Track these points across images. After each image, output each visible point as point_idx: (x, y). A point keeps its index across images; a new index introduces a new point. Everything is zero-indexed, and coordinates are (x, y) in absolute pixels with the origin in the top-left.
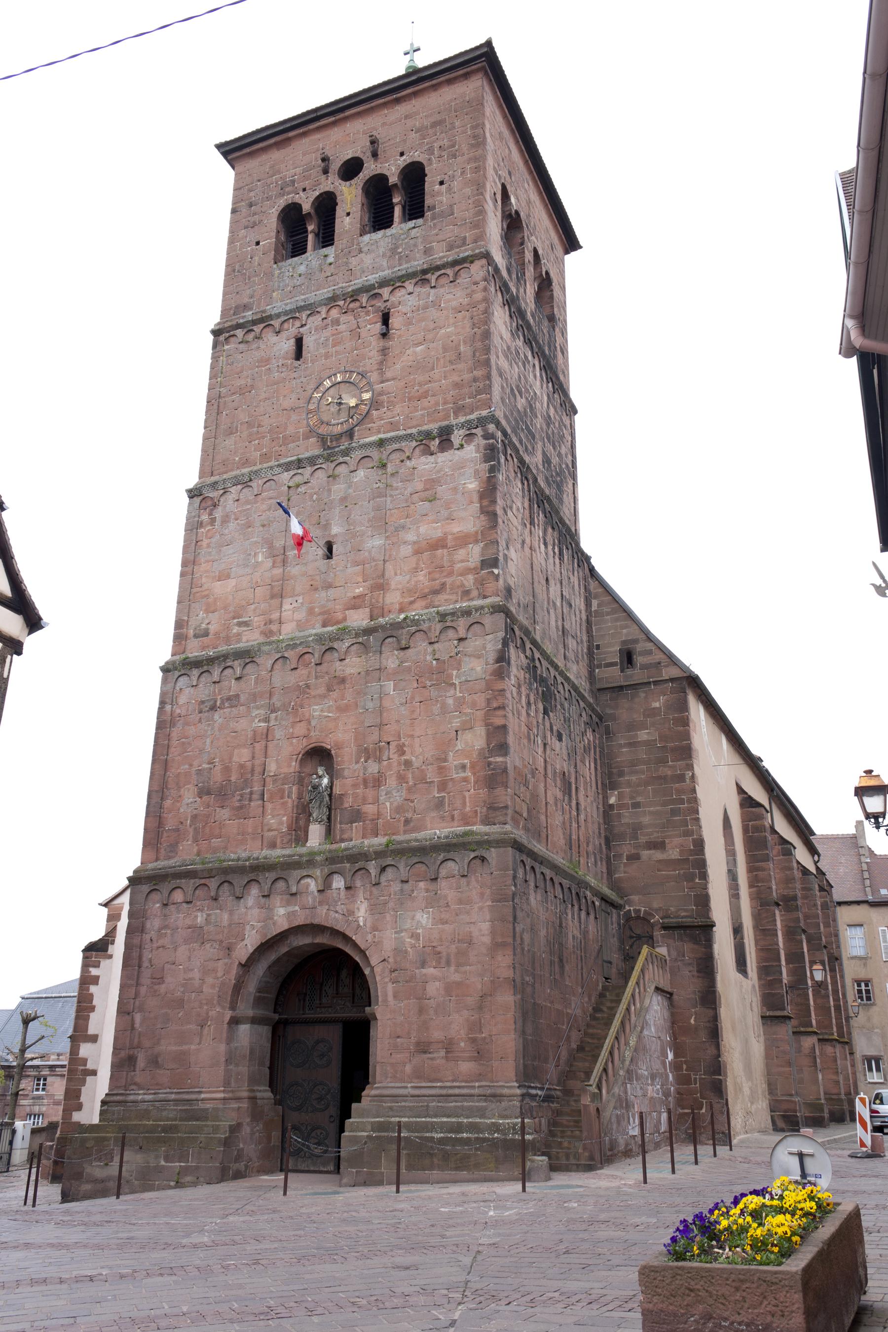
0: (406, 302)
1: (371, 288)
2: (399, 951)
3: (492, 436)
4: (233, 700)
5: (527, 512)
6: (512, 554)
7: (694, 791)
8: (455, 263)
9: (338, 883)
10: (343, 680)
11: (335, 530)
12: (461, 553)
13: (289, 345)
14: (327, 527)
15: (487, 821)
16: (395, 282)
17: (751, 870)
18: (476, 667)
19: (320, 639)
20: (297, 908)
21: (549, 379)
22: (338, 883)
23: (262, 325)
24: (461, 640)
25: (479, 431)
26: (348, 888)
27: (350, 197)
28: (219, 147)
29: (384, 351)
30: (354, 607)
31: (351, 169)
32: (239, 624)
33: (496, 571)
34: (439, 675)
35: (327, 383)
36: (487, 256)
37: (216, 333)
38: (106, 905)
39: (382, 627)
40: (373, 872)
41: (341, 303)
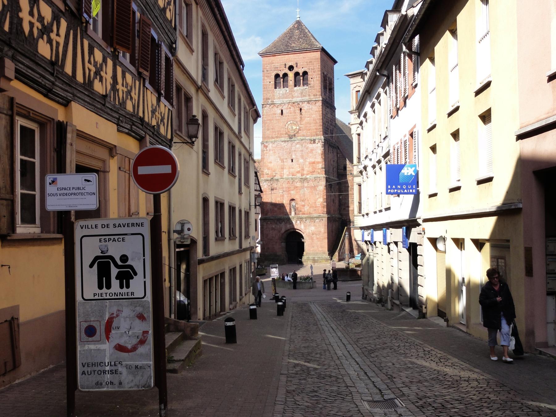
0: (305, 106)
2: (309, 233)
11: (294, 157)
12: (318, 165)
14: (291, 156)
16: (303, 102)
19: (292, 179)
22: (298, 222)
27: (291, 75)
29: (301, 118)
31: (291, 68)
34: (315, 187)
35: (289, 123)
37: (263, 105)
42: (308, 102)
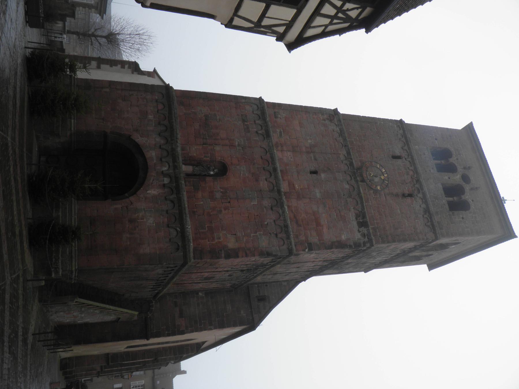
0: (417, 205)
1: (422, 189)
3: (364, 246)
4: (247, 129)
5: (329, 259)
6: (312, 255)
7: (205, 330)
8: (433, 225)
9: (166, 180)
10: (257, 180)
11: (323, 175)
13: (398, 153)
15: (195, 249)
16: (424, 200)
17: (170, 348)
18: (264, 243)
19: (275, 170)
20: (155, 161)
21: (380, 263)
22: (166, 180)
23: (405, 141)
24: (276, 235)
25: (366, 239)
26: (164, 185)
27: (456, 178)
28: (471, 124)
29: (397, 195)
30: (289, 184)
31: (466, 178)
32: (280, 132)
33: (307, 250)
36: (437, 239)
38: (155, 71)
39: (281, 199)
40: (172, 197)
41: (415, 176)
42: (427, 211)
